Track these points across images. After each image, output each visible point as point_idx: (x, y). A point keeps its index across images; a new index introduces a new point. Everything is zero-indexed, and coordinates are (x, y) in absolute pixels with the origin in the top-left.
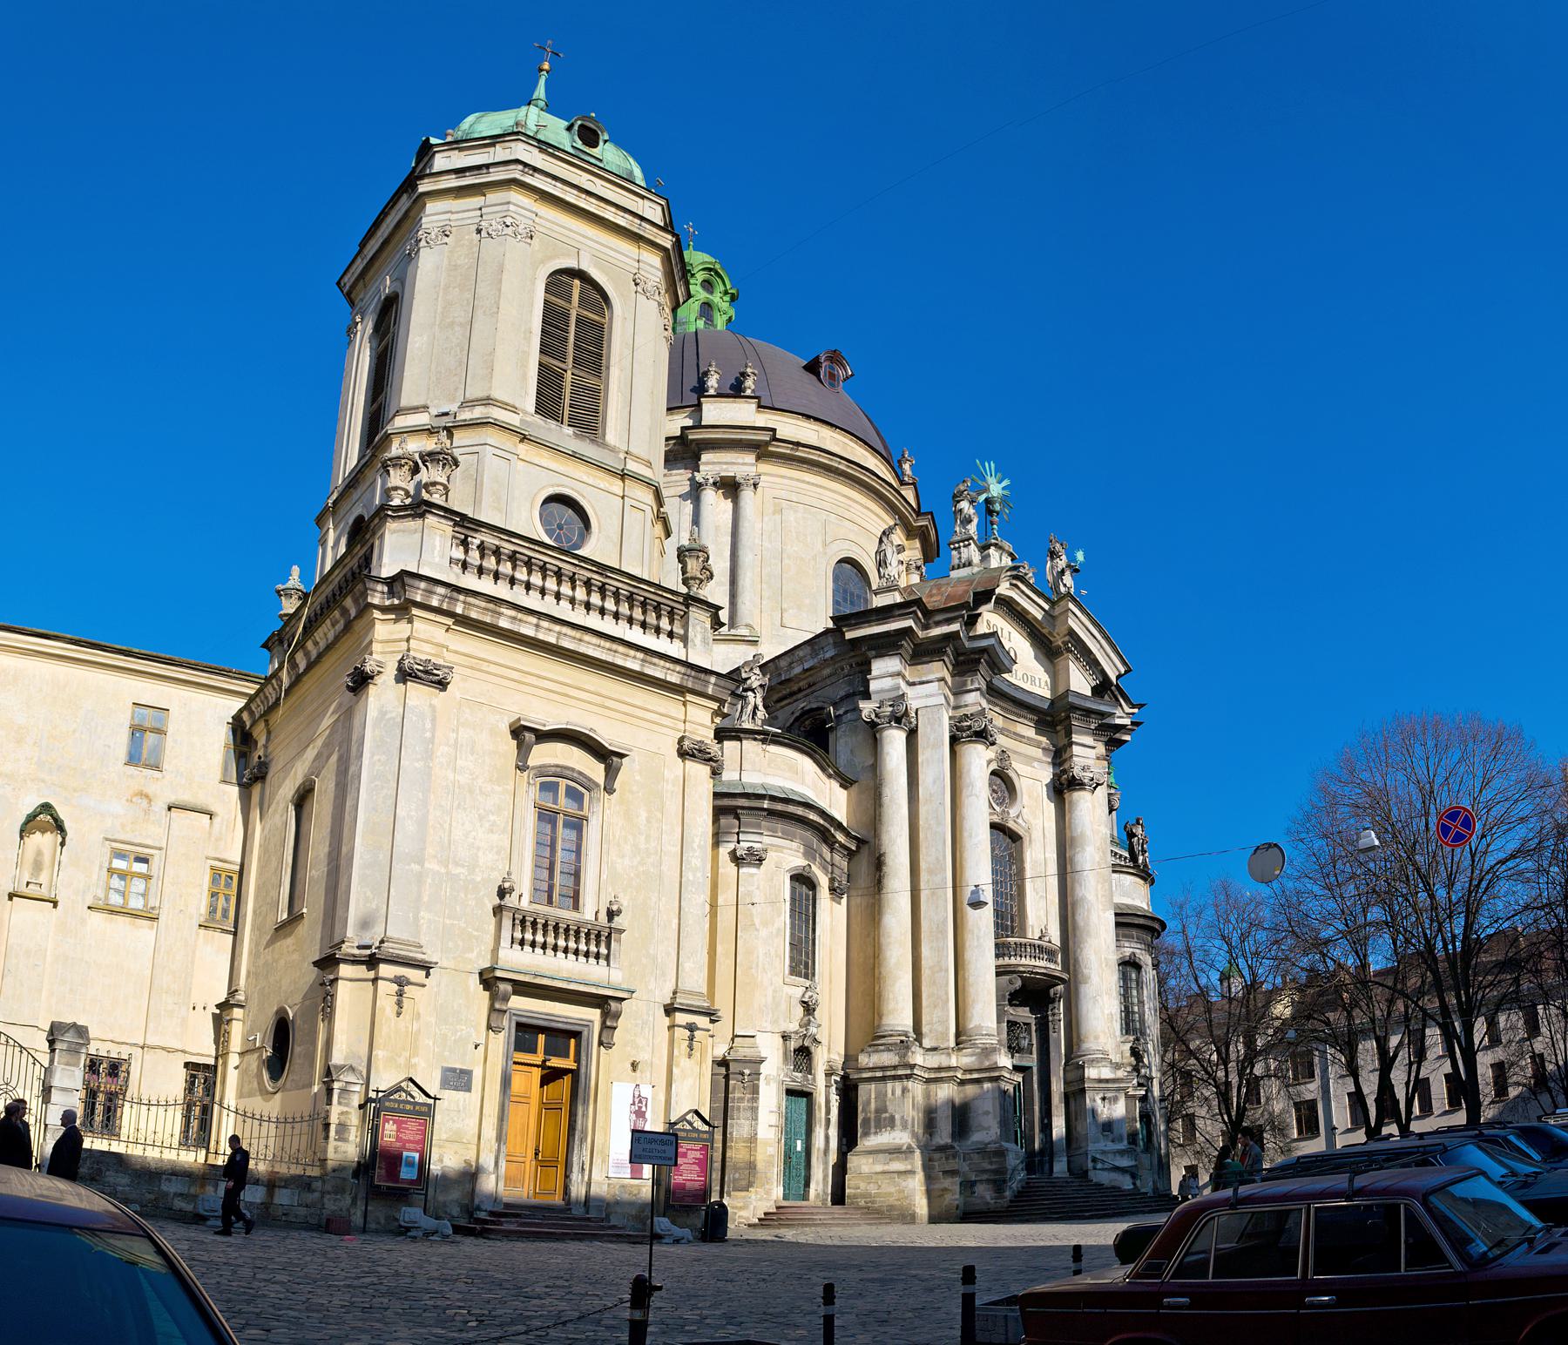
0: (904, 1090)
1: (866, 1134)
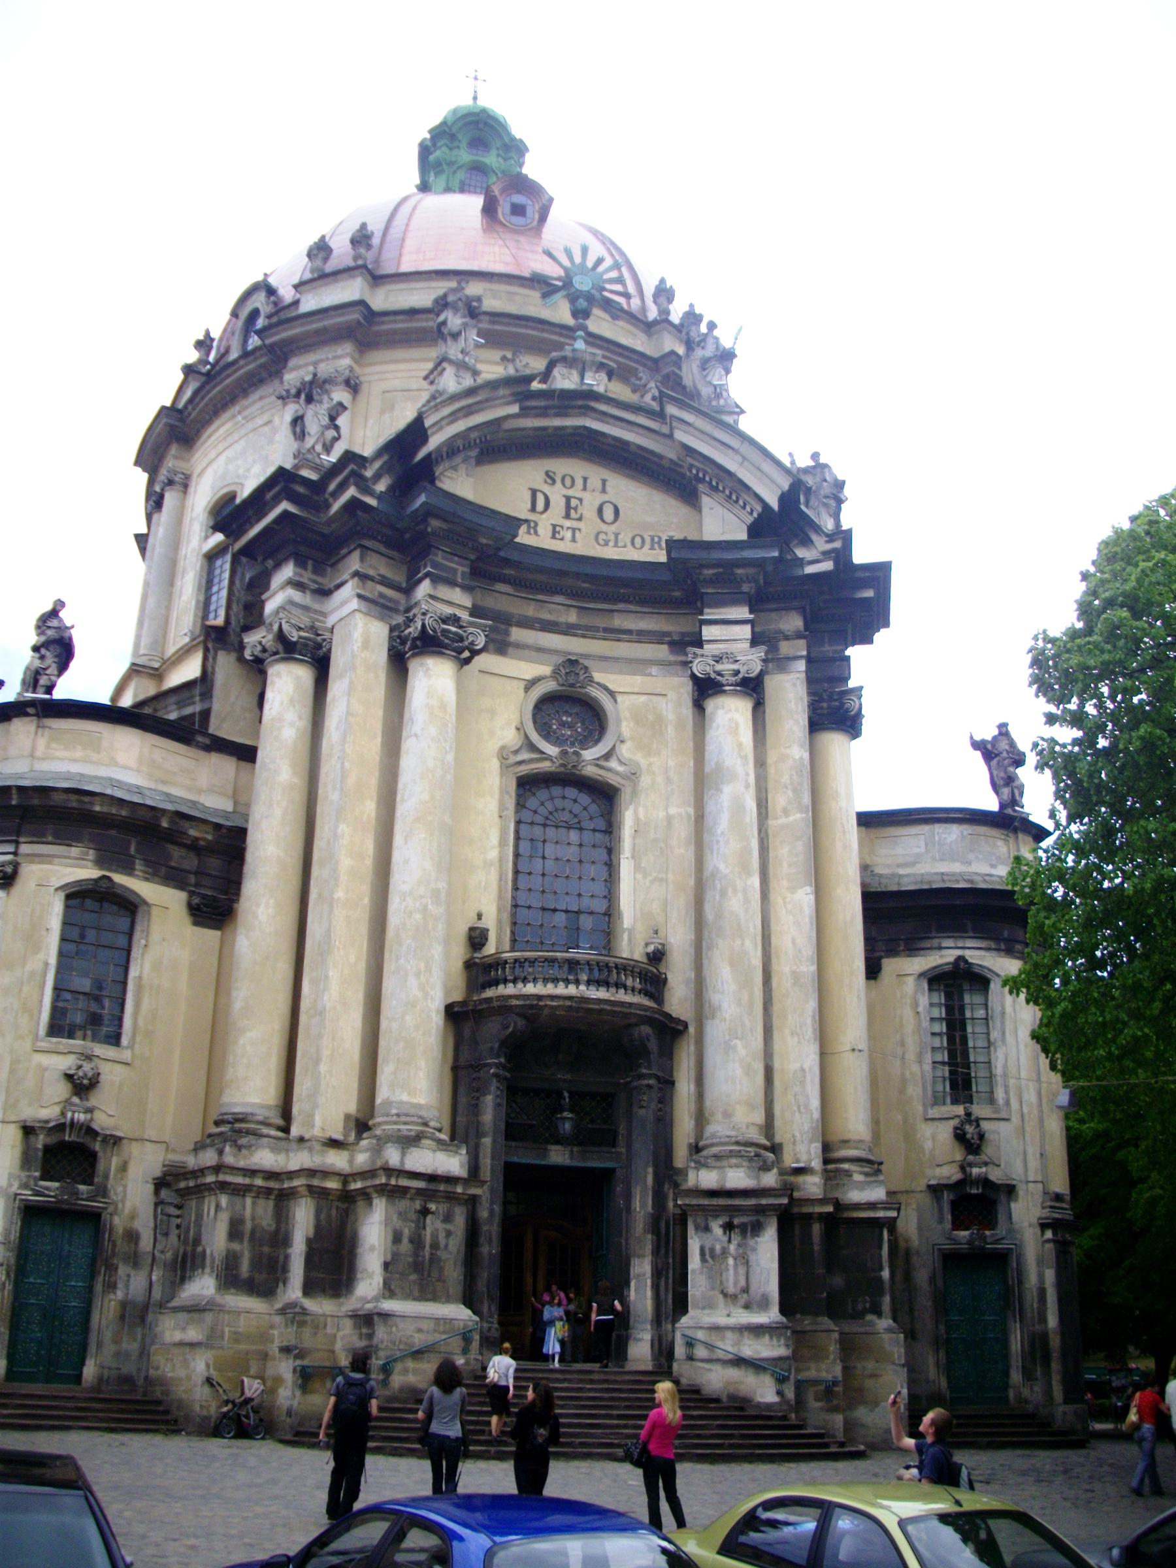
0: (218, 1206)
1: (183, 1280)
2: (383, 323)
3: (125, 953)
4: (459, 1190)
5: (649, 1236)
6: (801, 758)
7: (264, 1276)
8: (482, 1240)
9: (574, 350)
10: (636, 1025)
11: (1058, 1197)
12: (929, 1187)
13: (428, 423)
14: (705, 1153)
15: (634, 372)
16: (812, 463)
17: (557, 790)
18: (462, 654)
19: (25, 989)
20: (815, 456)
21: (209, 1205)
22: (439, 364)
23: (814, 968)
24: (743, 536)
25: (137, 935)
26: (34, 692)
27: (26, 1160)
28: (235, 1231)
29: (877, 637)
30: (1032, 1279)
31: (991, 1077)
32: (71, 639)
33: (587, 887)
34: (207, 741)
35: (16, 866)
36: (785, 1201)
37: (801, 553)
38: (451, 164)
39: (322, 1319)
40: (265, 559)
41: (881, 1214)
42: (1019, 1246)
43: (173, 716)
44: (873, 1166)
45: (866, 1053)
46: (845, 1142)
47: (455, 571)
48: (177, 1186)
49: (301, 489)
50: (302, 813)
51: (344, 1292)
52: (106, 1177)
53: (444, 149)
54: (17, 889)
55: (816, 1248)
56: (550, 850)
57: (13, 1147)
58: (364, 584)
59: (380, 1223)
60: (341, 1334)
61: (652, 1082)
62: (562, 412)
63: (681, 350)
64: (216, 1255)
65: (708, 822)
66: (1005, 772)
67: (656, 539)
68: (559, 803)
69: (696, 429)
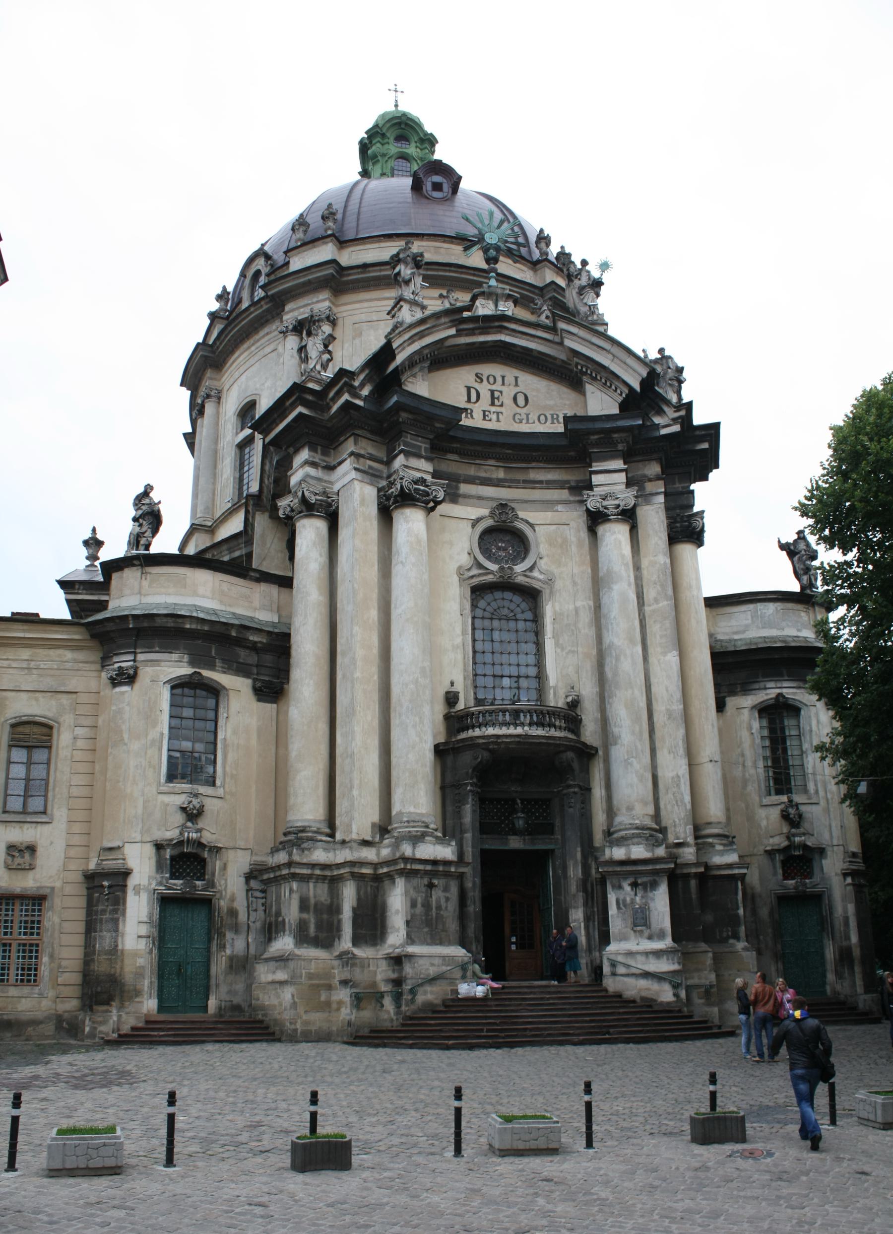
0: (291, 891)
1: (270, 940)
2: (349, 275)
3: (213, 724)
4: (453, 869)
5: (581, 894)
6: (665, 563)
7: (325, 935)
8: (469, 902)
9: (490, 287)
10: (565, 751)
11: (854, 855)
12: (766, 851)
13: (395, 346)
14: (615, 836)
15: (532, 301)
16: (659, 356)
17: (498, 594)
18: (430, 505)
19: (149, 752)
20: (661, 351)
21: (285, 889)
22: (398, 303)
23: (682, 707)
24: (616, 411)
25: (221, 710)
26: (137, 550)
27: (159, 867)
28: (304, 905)
29: (711, 475)
30: (839, 911)
31: (804, 775)
32: (159, 511)
33: (523, 659)
34: (258, 576)
35: (136, 669)
36: (672, 866)
37: (657, 420)
38: (384, 155)
39: (366, 961)
40: (288, 447)
41: (736, 871)
42: (830, 889)
43: (226, 558)
44: (728, 840)
45: (719, 763)
46: (710, 823)
47: (420, 447)
48: (260, 877)
49: (310, 398)
50: (327, 621)
51: (379, 941)
52: (213, 874)
53: (378, 145)
54: (137, 686)
55: (694, 896)
56: (496, 635)
57: (149, 859)
58: (358, 460)
59: (402, 895)
60: (380, 970)
61: (576, 790)
62: (485, 331)
63: (562, 282)
64: (292, 922)
65: (604, 610)
66: (804, 565)
67: (555, 416)
68: (500, 603)
69: (579, 337)
